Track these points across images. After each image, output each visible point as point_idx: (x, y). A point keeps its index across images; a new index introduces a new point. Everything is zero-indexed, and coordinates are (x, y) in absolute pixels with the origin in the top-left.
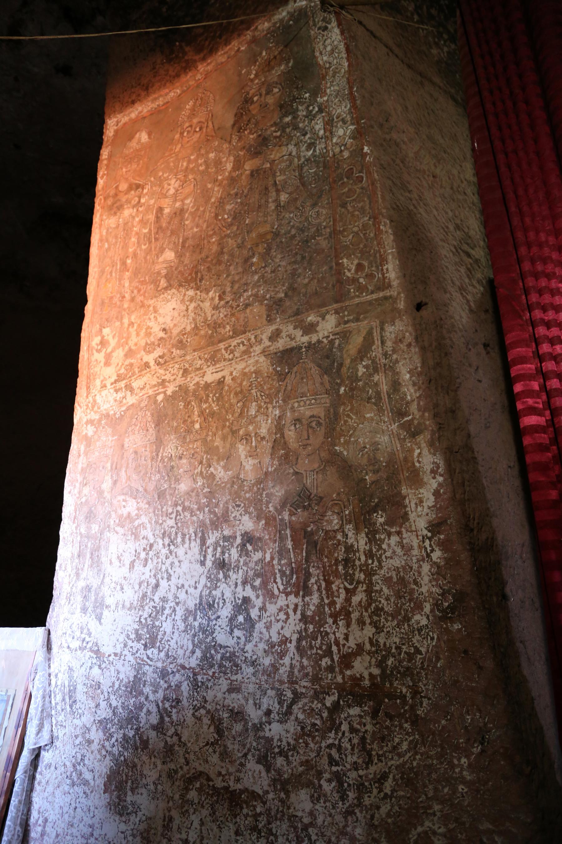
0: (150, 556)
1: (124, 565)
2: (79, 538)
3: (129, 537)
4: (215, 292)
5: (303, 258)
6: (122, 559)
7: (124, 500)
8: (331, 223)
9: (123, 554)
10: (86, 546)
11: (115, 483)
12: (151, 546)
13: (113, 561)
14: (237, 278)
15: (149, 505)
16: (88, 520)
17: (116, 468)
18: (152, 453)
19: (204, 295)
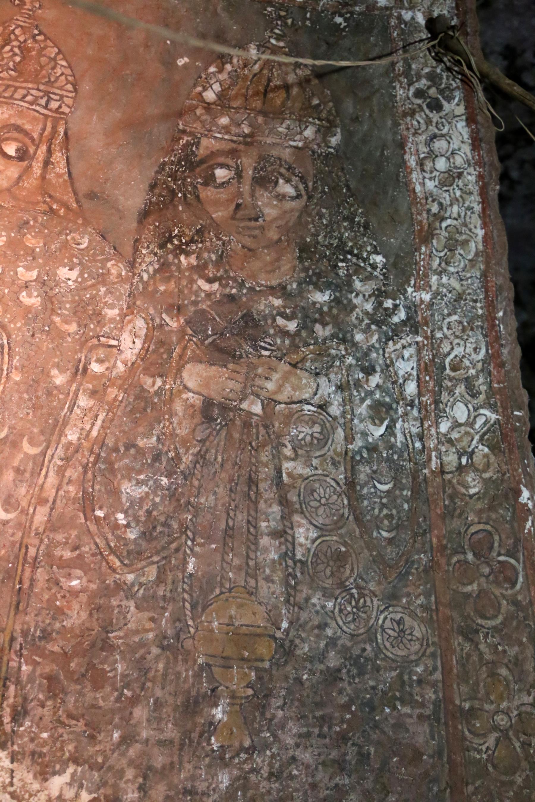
4: (76, 782)
5: (363, 758)
8: (438, 676)
14: (159, 760)
19: (29, 777)
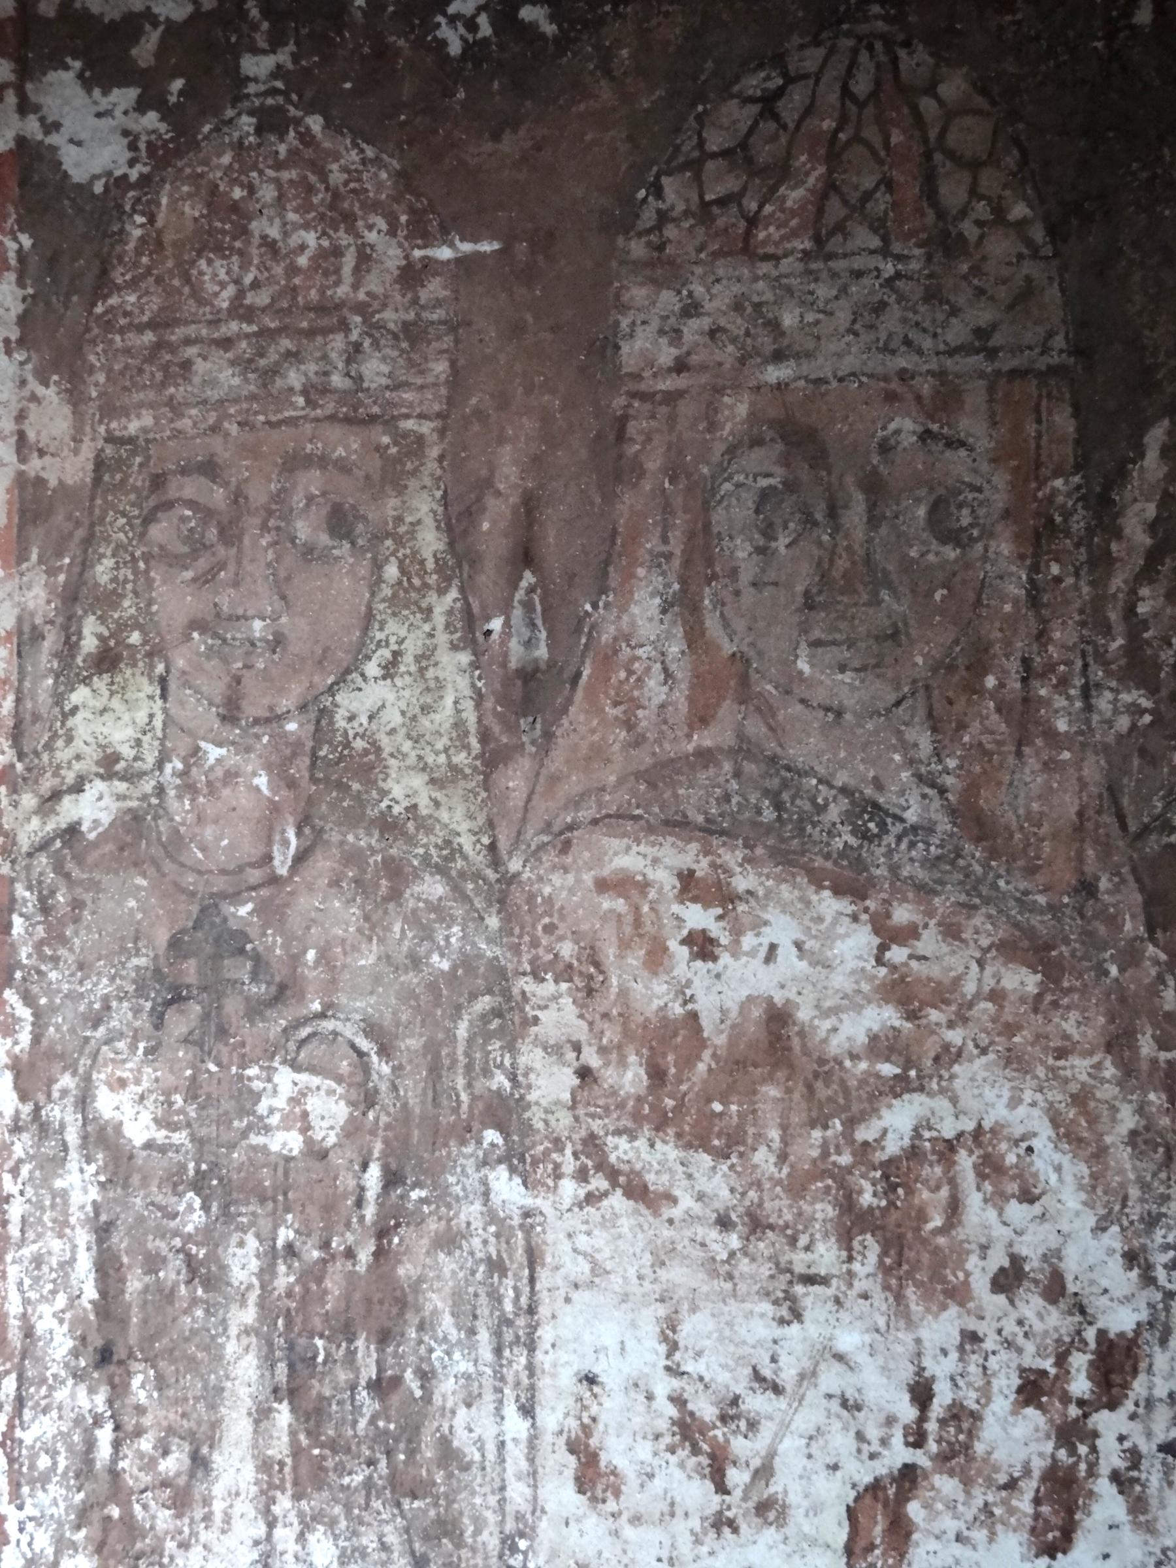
0: (1111, 1457)
1: (769, 1510)
2: (80, 1183)
3: (826, 1255)
6: (740, 1446)
7: (690, 886)
9: (756, 1402)
10: (206, 1274)
11: (527, 697)
12: (1116, 1363)
13: (618, 1452)
15: (1052, 971)
16: (179, 1023)
17: (526, 556)
18: (1030, 469)
